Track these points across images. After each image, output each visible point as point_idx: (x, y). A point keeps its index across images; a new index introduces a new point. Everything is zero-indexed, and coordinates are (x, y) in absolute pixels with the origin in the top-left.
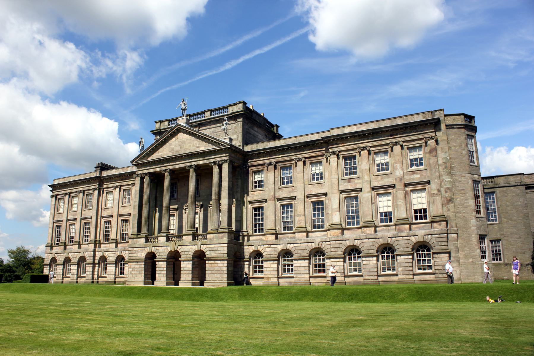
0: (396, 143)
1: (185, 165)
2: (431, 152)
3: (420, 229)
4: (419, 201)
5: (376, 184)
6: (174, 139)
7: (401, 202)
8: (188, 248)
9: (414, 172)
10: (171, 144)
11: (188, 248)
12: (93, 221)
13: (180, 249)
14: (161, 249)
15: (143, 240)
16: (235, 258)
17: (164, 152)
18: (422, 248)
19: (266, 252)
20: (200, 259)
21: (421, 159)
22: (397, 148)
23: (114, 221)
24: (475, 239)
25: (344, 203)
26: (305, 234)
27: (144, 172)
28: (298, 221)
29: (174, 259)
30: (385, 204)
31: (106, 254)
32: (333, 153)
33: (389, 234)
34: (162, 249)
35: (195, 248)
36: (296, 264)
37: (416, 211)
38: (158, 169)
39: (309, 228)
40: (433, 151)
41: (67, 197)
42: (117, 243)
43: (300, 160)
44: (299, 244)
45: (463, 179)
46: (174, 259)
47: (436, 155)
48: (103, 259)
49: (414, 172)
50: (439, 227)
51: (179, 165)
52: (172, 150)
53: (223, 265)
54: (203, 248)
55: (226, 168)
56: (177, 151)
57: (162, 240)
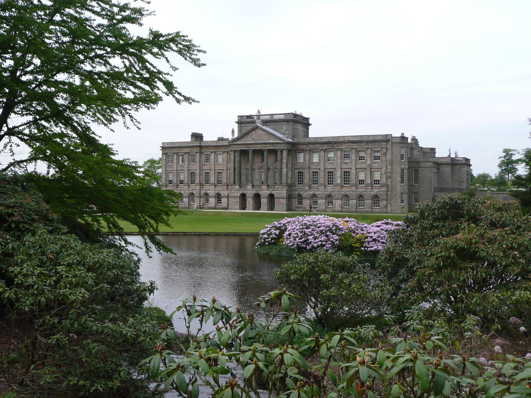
0: (369, 148)
1: (261, 148)
2: (383, 154)
3: (376, 189)
4: (377, 176)
5: (358, 167)
6: (254, 132)
7: (368, 176)
8: (265, 192)
9: (375, 163)
10: (252, 135)
11: (265, 192)
12: (198, 172)
13: (260, 193)
14: (249, 192)
15: (237, 187)
16: (289, 198)
17: (248, 140)
18: (376, 198)
19: (304, 194)
20: (271, 197)
21: (379, 157)
22: (369, 151)
23: (212, 174)
24: (399, 195)
25: (343, 174)
26: (323, 187)
27: (236, 149)
28: (321, 180)
29: (257, 197)
30: (362, 176)
31: (208, 192)
32: (339, 149)
33: (362, 190)
34: (250, 192)
35: (269, 192)
36: (319, 201)
37: (375, 181)
38: (245, 149)
39: (326, 184)
40: (385, 154)
41: (175, 155)
42: (215, 186)
43: (322, 150)
44: (320, 191)
45: (396, 168)
46: (257, 197)
47: (386, 156)
48: (207, 194)
49: (375, 163)
50: (384, 189)
51: (258, 147)
52: (253, 138)
53: (284, 201)
54: (273, 192)
55: (285, 153)
56: (257, 140)
57: (250, 187)
